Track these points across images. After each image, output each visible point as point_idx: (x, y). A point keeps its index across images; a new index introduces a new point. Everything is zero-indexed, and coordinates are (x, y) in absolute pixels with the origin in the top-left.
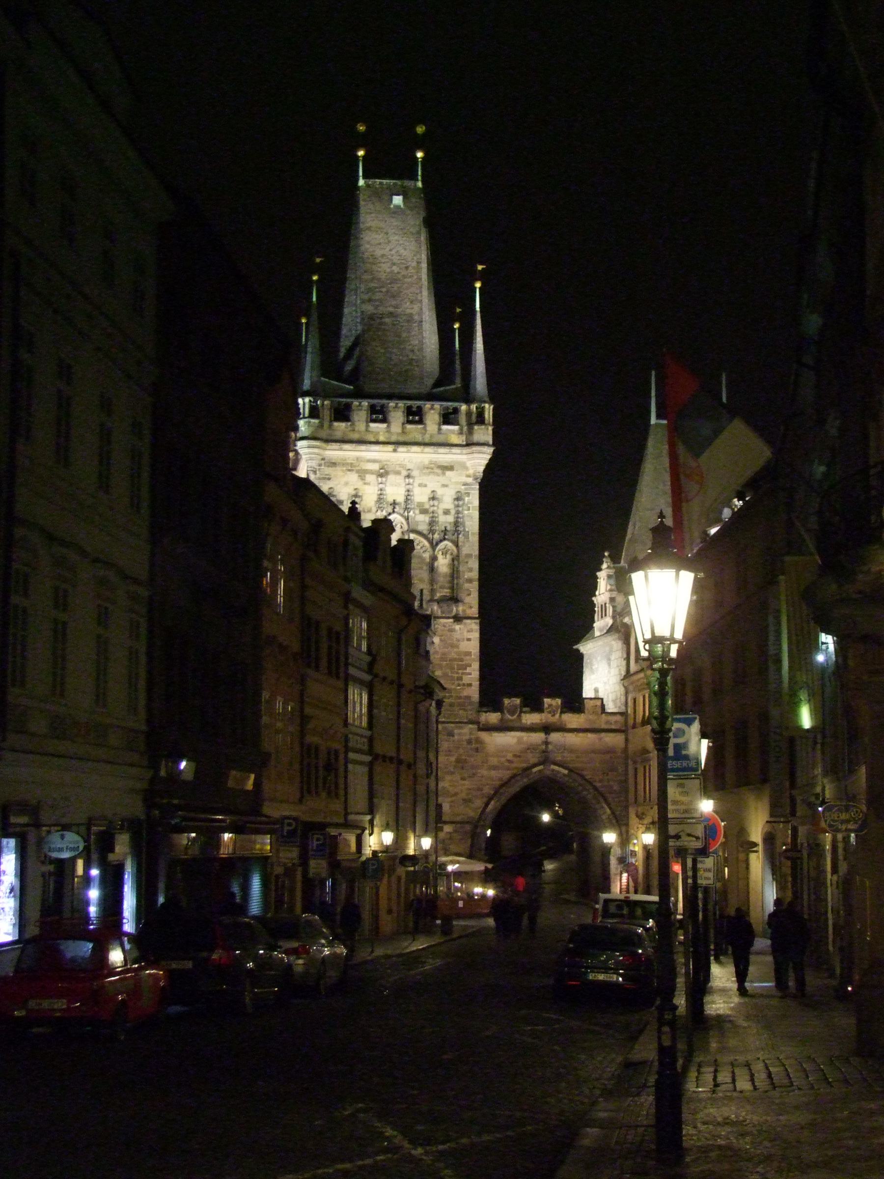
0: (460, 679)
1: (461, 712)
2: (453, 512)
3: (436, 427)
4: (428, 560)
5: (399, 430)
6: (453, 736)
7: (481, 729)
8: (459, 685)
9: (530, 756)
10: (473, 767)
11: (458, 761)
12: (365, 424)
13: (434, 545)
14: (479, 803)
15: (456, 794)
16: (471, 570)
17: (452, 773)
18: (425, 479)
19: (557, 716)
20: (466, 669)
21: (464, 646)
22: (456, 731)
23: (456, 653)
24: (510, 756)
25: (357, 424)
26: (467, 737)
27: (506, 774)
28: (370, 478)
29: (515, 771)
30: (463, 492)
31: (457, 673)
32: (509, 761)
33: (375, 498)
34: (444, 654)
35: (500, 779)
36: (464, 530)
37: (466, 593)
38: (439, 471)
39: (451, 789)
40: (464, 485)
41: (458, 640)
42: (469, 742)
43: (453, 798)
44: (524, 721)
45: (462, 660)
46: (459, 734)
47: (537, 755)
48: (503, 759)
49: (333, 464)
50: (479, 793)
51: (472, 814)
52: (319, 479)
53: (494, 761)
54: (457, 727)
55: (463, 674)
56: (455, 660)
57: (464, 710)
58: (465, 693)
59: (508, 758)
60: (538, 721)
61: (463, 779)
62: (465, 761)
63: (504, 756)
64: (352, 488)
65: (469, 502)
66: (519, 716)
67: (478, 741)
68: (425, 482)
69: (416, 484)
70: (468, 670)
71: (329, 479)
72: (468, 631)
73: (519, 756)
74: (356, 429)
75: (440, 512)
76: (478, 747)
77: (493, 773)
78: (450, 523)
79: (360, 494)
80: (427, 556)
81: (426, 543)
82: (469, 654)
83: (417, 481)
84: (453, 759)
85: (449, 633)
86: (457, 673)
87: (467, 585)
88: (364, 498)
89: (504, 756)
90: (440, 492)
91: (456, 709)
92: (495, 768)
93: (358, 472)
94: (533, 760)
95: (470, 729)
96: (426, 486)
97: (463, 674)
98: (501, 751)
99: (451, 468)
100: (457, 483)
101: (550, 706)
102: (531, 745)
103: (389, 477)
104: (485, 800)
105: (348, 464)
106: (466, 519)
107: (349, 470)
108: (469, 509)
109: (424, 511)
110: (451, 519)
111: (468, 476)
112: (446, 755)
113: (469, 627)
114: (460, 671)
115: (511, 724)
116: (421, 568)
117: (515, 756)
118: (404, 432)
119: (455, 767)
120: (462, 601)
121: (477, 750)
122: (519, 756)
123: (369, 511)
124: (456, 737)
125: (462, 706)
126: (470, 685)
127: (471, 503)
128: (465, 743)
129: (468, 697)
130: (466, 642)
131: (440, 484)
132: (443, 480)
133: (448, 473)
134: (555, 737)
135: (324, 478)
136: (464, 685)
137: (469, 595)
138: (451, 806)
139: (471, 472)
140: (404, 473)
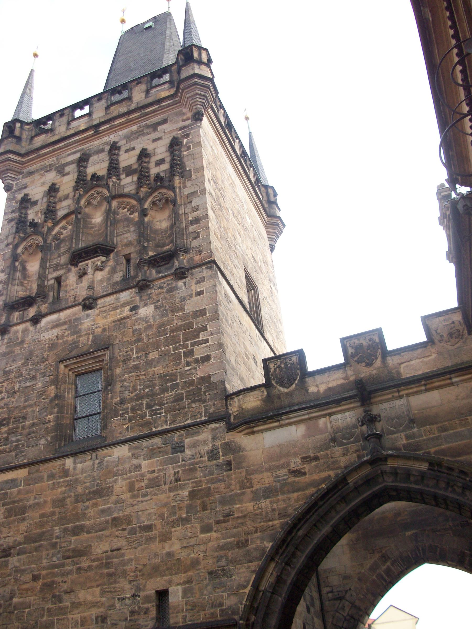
0: (191, 353)
1: (194, 405)
2: (168, 159)
3: (143, 95)
4: (136, 219)
5: (103, 114)
6: (183, 451)
7: (231, 428)
8: (188, 364)
9: (338, 450)
10: (223, 502)
11: (193, 495)
12: (66, 125)
13: (141, 201)
14: (244, 575)
15: (195, 563)
16: (196, 209)
17: (186, 521)
18: (132, 144)
19: (378, 363)
20: (198, 336)
21: (191, 306)
22: (187, 441)
23: (179, 318)
24: (295, 462)
25: (57, 129)
26: (210, 447)
27: (295, 502)
28: (67, 169)
29: (313, 490)
30: (179, 136)
31: (185, 346)
32: (297, 473)
33: (73, 184)
34: (162, 325)
35: (282, 515)
36: (185, 170)
37: (193, 236)
38: (151, 130)
39: (183, 555)
40: (181, 129)
41: (184, 299)
42: (213, 455)
43: (190, 573)
44: (312, 389)
45: (190, 326)
46: (194, 445)
47: (353, 447)
48: (282, 472)
49: (32, 173)
50: (241, 552)
51: (230, 601)
52: (16, 191)
53: (266, 479)
54: (187, 436)
55: (193, 345)
56: (179, 328)
57: (199, 401)
58: (200, 374)
59: (292, 466)
60: (342, 381)
61: (206, 529)
62: (208, 493)
63: (282, 466)
64: (50, 184)
65: (187, 143)
66: (303, 385)
67: (230, 448)
68: (132, 146)
69: (122, 152)
70: (202, 336)
71: (25, 188)
72: (198, 283)
73: (316, 458)
74: (57, 132)
75: (152, 165)
76: (230, 460)
77: (265, 504)
78: (165, 171)
79: (57, 187)
80: (135, 216)
81: (134, 202)
82: (202, 312)
83: (123, 149)
84: (186, 493)
85: (167, 295)
86: (185, 346)
87: (191, 228)
88: (61, 189)
89: (282, 466)
90: (150, 147)
91: (185, 402)
92: (268, 493)
93: (56, 169)
94: (343, 461)
95: (214, 430)
96: (134, 149)
97: (192, 345)
98: (279, 456)
99: (165, 121)
100: (170, 132)
101: (359, 348)
102: (336, 430)
103: (91, 159)
104: (255, 565)
105: (47, 167)
106: (185, 160)
107: (47, 171)
108: (189, 148)
109: (129, 171)
110: (165, 167)
111: (184, 121)
112: (171, 490)
113: (200, 275)
114: (189, 343)
115: (285, 401)
116: (128, 231)
117: (306, 459)
118: (106, 114)
119: (190, 508)
120: (187, 251)
121: (229, 464)
122: (316, 458)
123: (66, 197)
124: (188, 452)
125: (195, 396)
126: (207, 358)
127: (193, 142)
128: (206, 458)
129: (206, 379)
130: (196, 299)
131: (151, 141)
132: (154, 135)
133: (160, 128)
134: (388, 407)
135: (20, 189)
136: (196, 361)
137: (195, 238)
138: (185, 592)
139: (189, 115)
140: (108, 148)
